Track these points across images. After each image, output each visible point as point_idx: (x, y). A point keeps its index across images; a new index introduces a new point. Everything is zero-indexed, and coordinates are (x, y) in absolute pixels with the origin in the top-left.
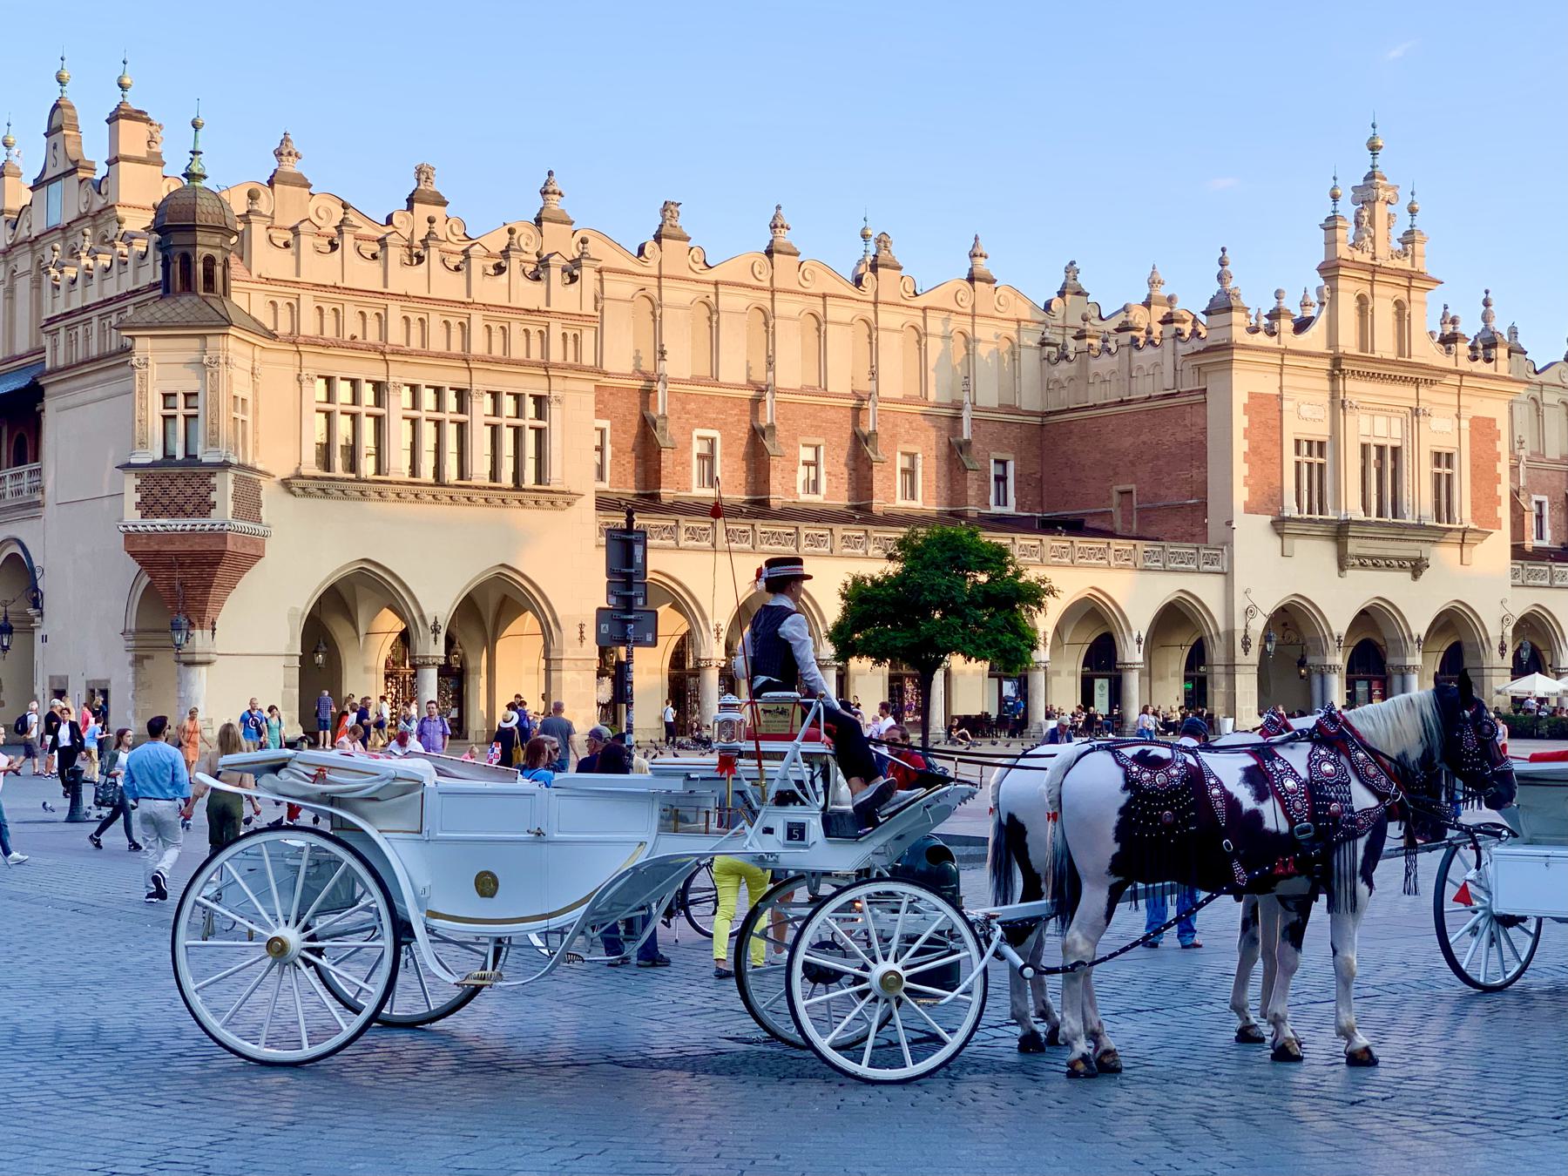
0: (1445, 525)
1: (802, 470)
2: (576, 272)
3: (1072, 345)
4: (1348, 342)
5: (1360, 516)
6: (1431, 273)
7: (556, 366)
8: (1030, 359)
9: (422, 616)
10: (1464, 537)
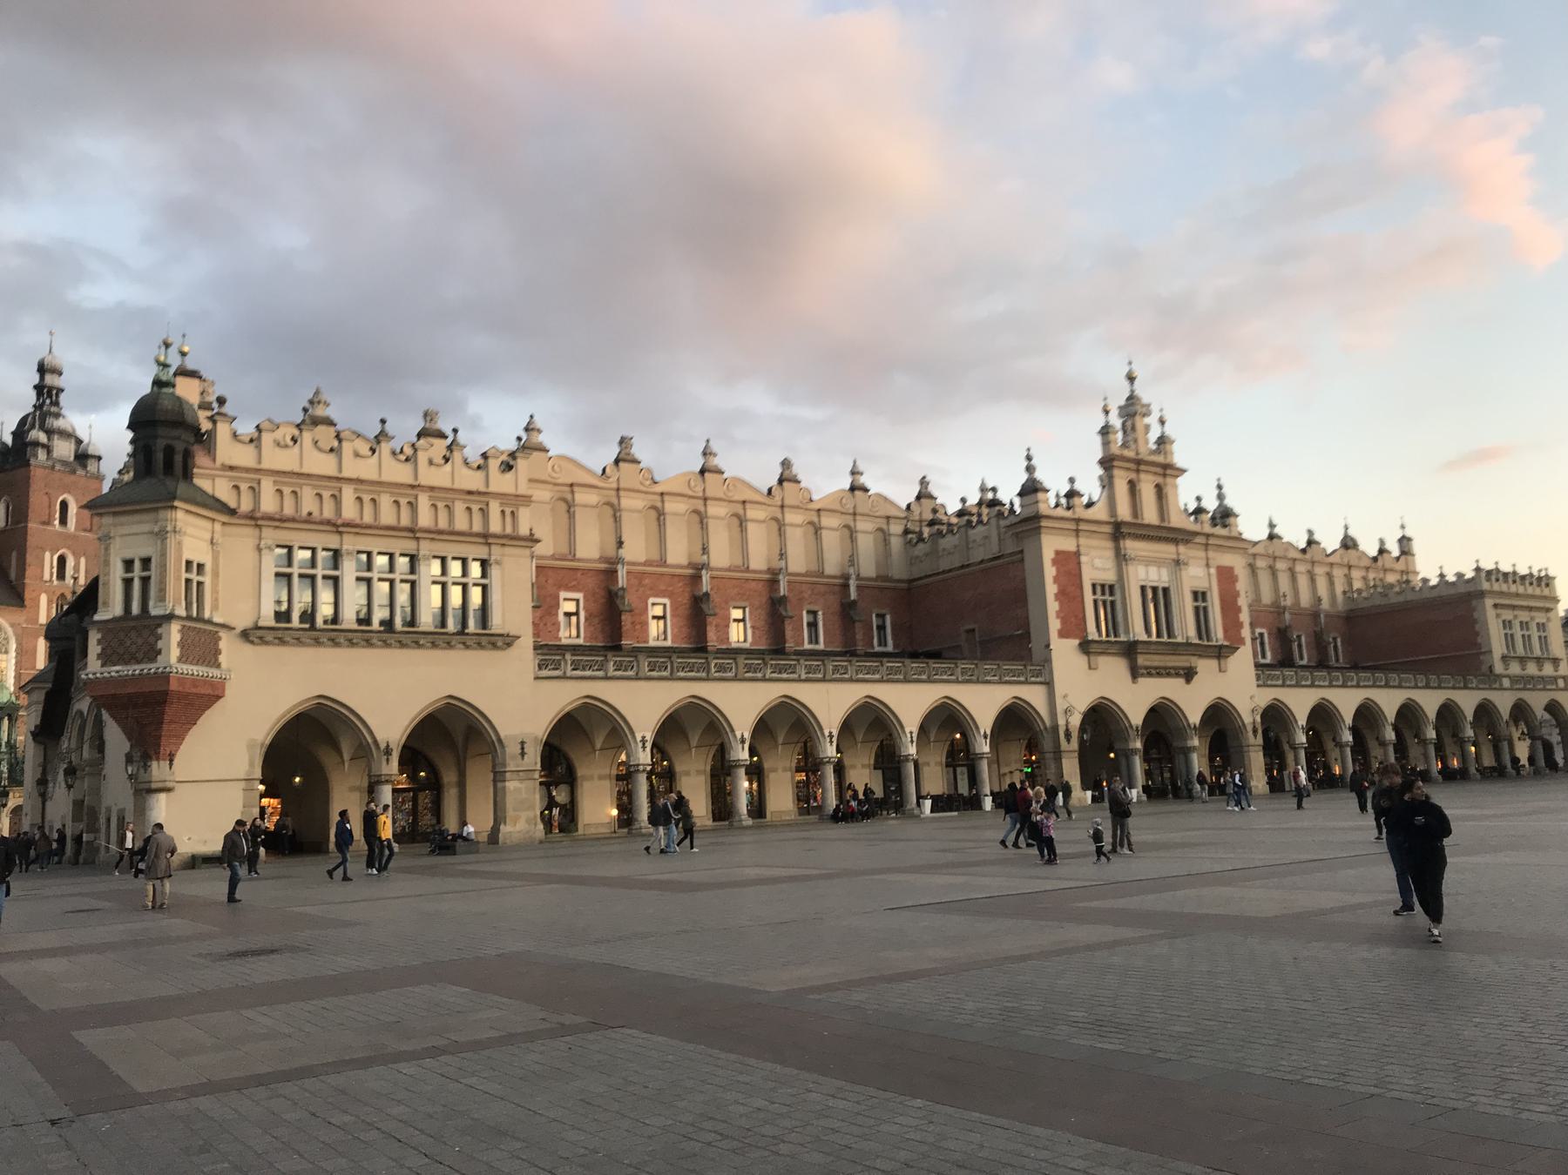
0: (1206, 643)
2: (512, 463)
4: (1124, 513)
5: (1144, 637)
7: (495, 536)
10: (1221, 653)
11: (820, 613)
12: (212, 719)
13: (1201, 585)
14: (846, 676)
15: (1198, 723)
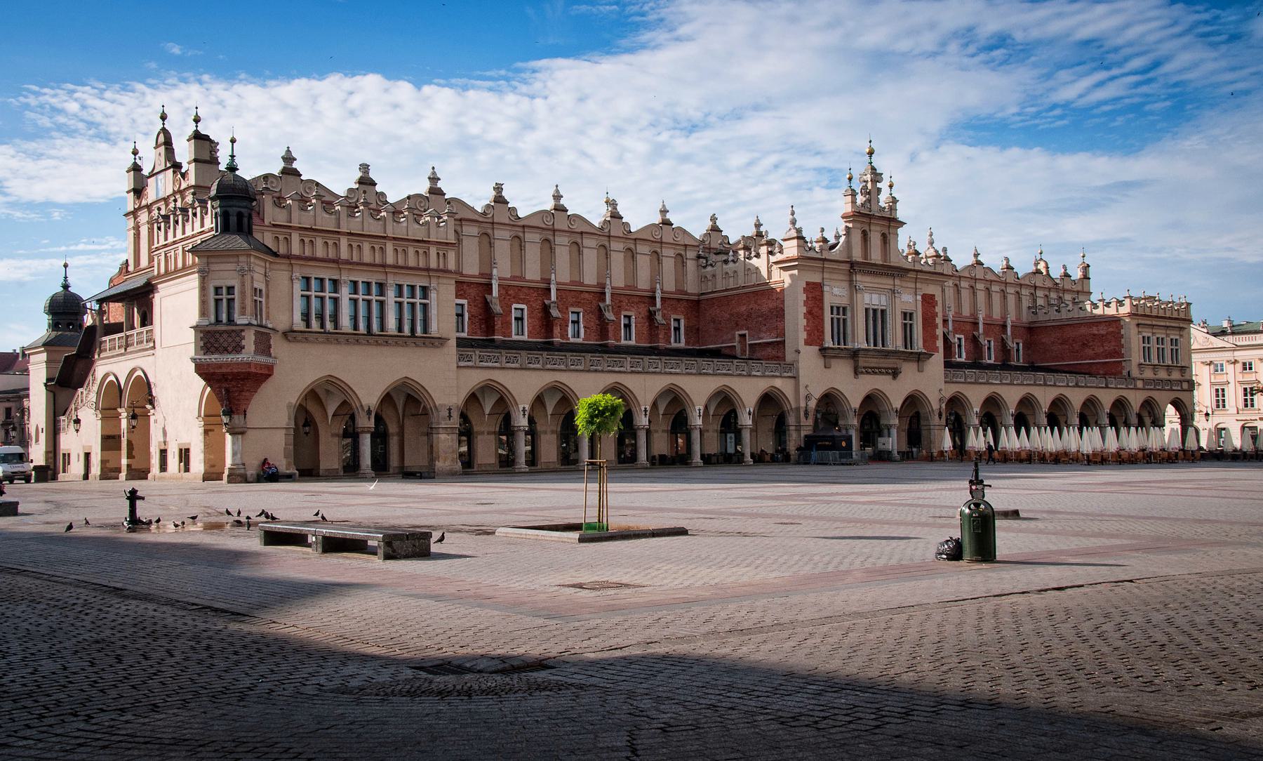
0: (910, 350)
5: (865, 346)
8: (691, 265)
10: (920, 358)
12: (267, 388)
13: (909, 309)
14: (657, 370)
15: (899, 407)
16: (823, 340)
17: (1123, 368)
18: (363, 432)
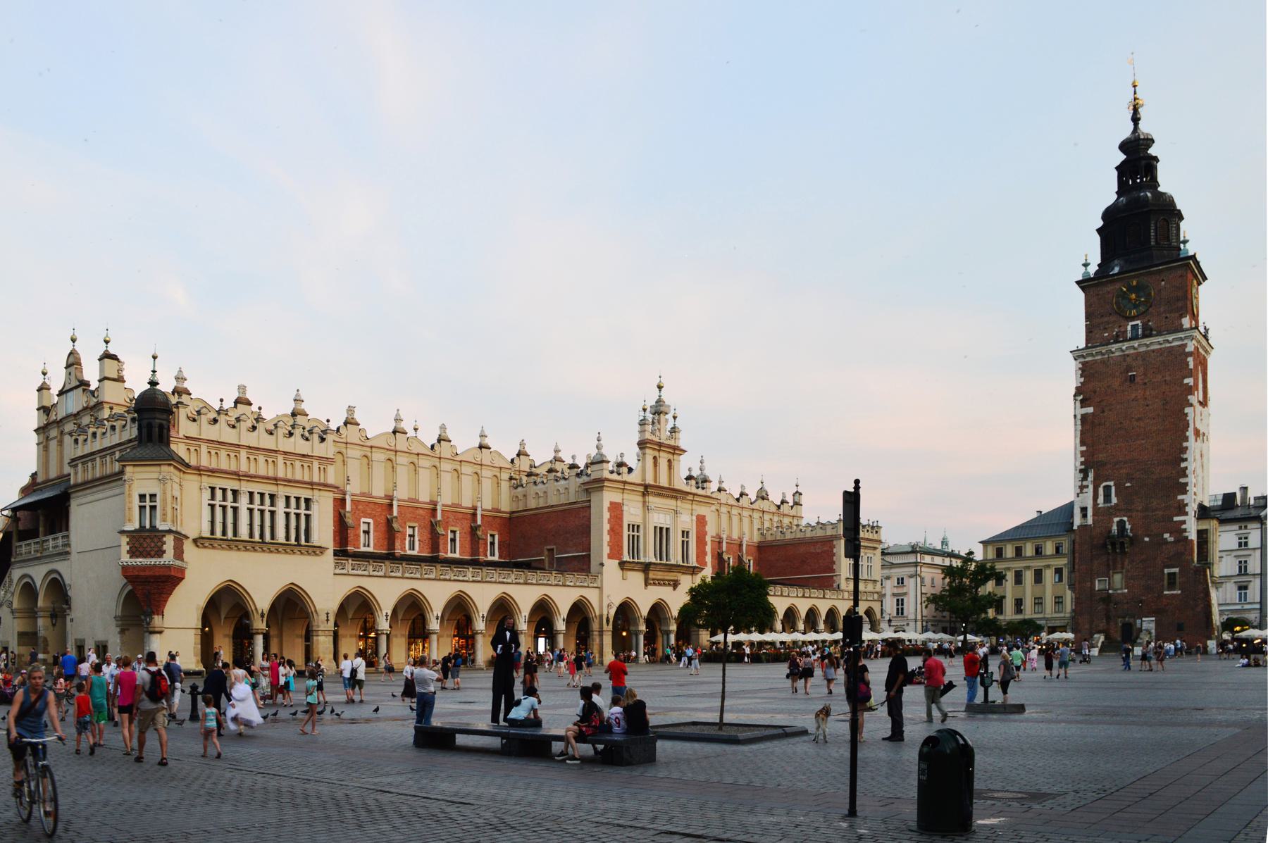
1: (408, 539)
3: (525, 479)
5: (653, 560)
6: (683, 447)
8: (505, 486)
9: (256, 609)
11: (458, 532)
16: (622, 554)
17: (834, 582)
18: (258, 633)
